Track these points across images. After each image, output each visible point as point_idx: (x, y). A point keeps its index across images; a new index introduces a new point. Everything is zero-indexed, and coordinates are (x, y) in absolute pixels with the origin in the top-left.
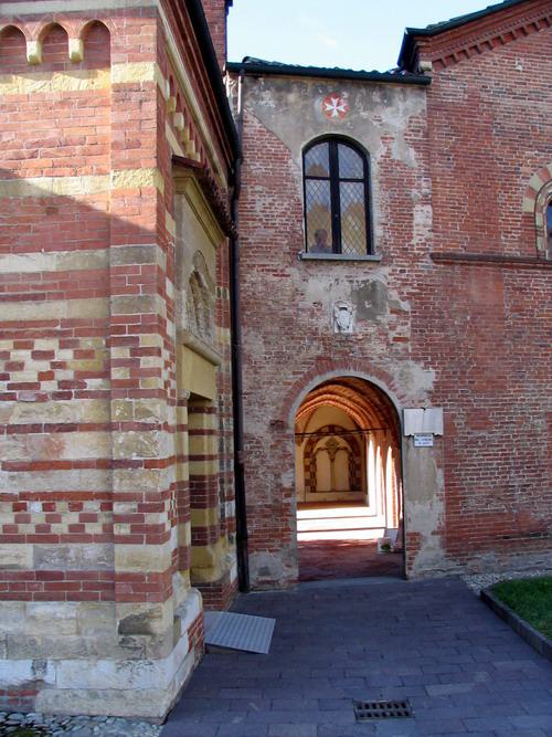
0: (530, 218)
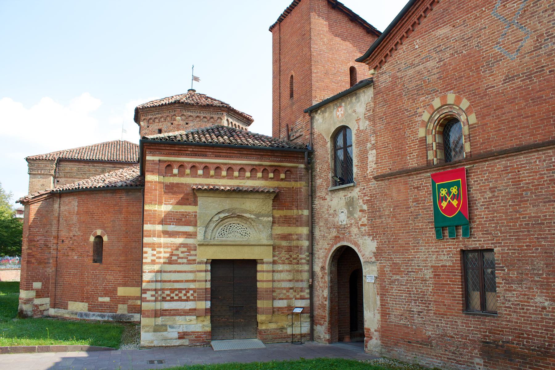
0: (424, 140)
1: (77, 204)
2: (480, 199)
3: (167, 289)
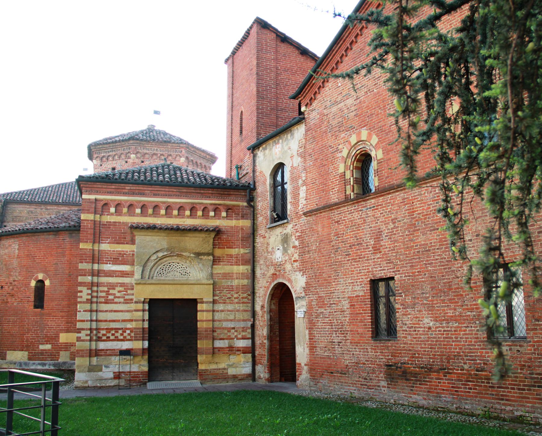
0: (344, 174)
1: (17, 247)
2: (385, 230)
3: (103, 329)
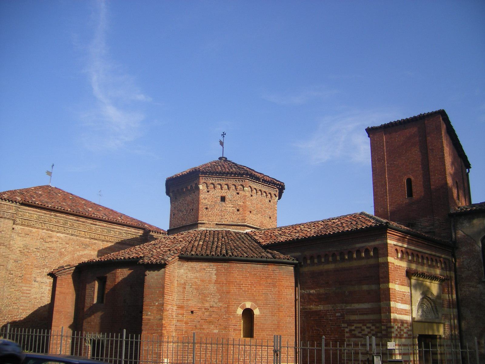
1: (215, 272)
